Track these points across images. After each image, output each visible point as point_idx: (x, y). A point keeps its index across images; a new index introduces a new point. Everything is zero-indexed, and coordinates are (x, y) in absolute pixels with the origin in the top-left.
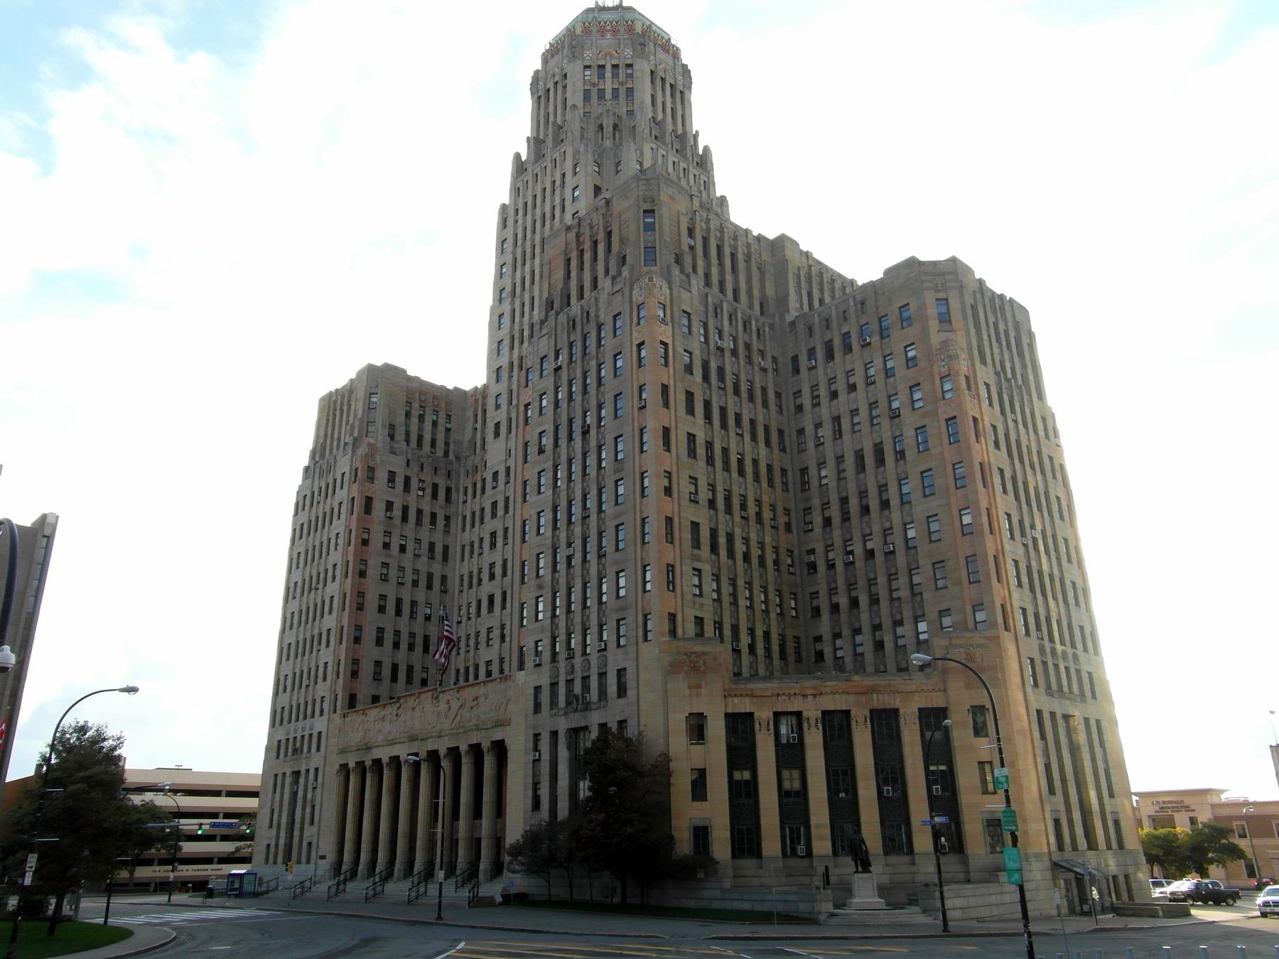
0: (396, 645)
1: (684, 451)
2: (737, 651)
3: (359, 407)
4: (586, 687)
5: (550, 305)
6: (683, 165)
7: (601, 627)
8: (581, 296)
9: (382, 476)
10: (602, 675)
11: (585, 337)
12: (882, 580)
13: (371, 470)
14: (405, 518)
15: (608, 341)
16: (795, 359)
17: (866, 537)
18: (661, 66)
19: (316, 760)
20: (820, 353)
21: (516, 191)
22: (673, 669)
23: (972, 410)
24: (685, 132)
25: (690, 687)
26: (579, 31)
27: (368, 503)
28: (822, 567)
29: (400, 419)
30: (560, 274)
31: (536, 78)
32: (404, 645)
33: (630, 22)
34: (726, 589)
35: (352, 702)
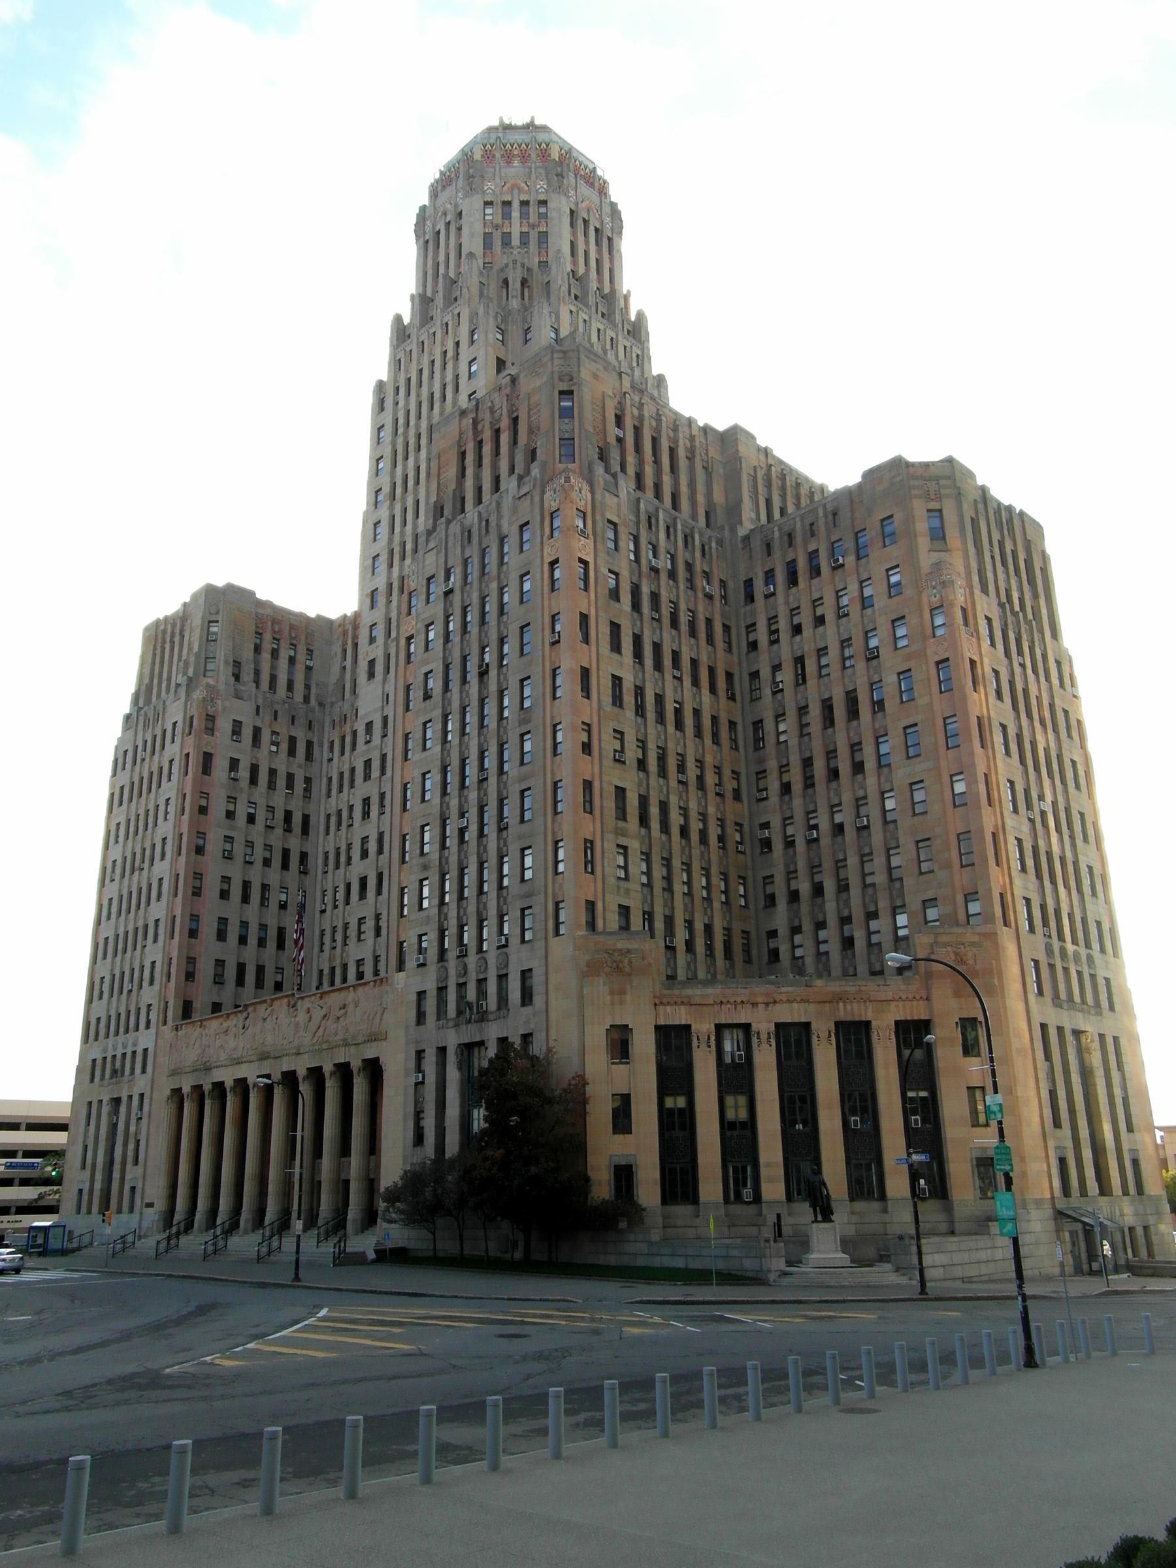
0: (243, 940)
1: (607, 699)
2: (671, 949)
3: (194, 638)
4: (482, 993)
5: (439, 510)
6: (610, 333)
7: (501, 858)
8: (479, 500)
9: (224, 726)
10: (502, 978)
11: (483, 553)
12: (853, 861)
13: (211, 718)
14: (254, 781)
15: (513, 559)
16: (749, 583)
17: (833, 808)
18: (584, 204)
20: (780, 577)
21: (396, 364)
22: (591, 970)
23: (968, 650)
24: (613, 291)
25: (612, 993)
26: (477, 156)
27: (207, 761)
29: (248, 654)
30: (452, 472)
31: (423, 215)
32: (253, 940)
33: (543, 145)
34: (658, 872)
35: (187, 1010)
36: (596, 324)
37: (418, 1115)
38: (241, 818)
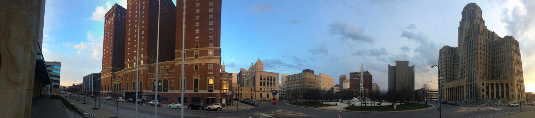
1: (482, 55)
2: (487, 76)
3: (444, 51)
4: (472, 80)
5: (466, 38)
6: (481, 22)
8: (470, 37)
9: (448, 57)
10: (473, 78)
11: (471, 41)
12: (502, 70)
14: (450, 62)
15: (474, 42)
16: (494, 46)
17: (501, 65)
19: (443, 88)
20: (497, 45)
21: (460, 25)
22: (481, 78)
23: (513, 53)
24: (482, 18)
26: (467, 6)
27: (446, 60)
28: (496, 68)
29: (449, 51)
30: (467, 34)
31: (462, 12)
34: (486, 70)
35: (447, 81)
36: (480, 21)
37: (467, 90)
38: (450, 65)
